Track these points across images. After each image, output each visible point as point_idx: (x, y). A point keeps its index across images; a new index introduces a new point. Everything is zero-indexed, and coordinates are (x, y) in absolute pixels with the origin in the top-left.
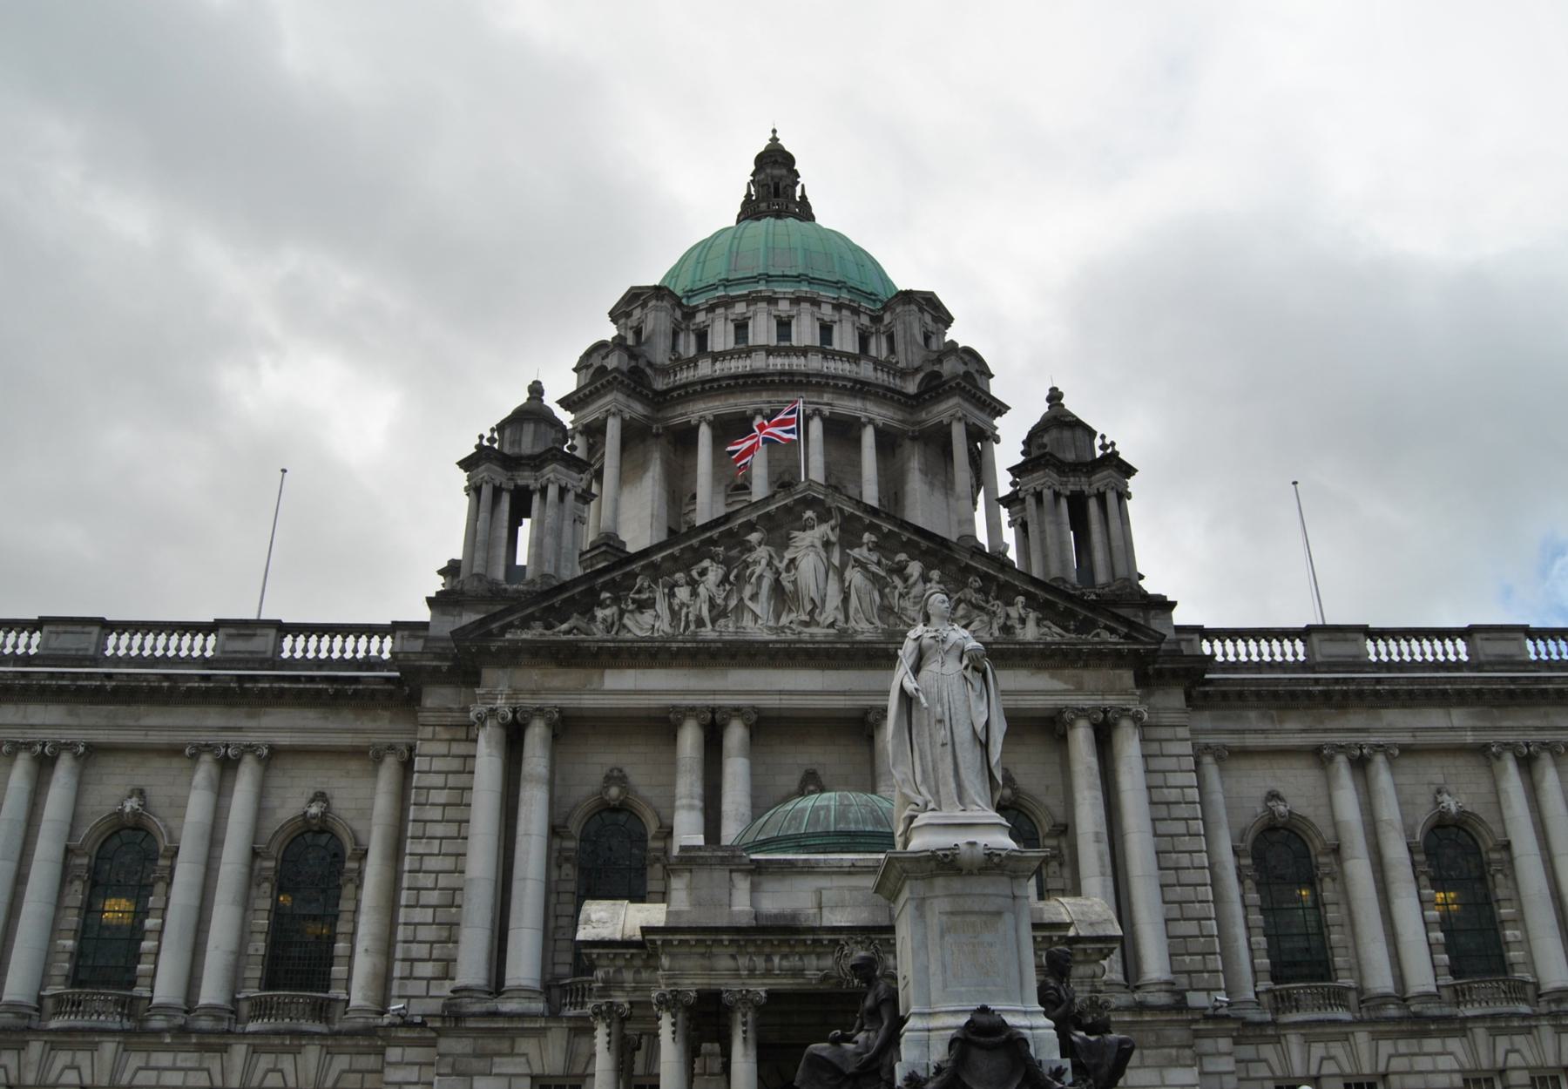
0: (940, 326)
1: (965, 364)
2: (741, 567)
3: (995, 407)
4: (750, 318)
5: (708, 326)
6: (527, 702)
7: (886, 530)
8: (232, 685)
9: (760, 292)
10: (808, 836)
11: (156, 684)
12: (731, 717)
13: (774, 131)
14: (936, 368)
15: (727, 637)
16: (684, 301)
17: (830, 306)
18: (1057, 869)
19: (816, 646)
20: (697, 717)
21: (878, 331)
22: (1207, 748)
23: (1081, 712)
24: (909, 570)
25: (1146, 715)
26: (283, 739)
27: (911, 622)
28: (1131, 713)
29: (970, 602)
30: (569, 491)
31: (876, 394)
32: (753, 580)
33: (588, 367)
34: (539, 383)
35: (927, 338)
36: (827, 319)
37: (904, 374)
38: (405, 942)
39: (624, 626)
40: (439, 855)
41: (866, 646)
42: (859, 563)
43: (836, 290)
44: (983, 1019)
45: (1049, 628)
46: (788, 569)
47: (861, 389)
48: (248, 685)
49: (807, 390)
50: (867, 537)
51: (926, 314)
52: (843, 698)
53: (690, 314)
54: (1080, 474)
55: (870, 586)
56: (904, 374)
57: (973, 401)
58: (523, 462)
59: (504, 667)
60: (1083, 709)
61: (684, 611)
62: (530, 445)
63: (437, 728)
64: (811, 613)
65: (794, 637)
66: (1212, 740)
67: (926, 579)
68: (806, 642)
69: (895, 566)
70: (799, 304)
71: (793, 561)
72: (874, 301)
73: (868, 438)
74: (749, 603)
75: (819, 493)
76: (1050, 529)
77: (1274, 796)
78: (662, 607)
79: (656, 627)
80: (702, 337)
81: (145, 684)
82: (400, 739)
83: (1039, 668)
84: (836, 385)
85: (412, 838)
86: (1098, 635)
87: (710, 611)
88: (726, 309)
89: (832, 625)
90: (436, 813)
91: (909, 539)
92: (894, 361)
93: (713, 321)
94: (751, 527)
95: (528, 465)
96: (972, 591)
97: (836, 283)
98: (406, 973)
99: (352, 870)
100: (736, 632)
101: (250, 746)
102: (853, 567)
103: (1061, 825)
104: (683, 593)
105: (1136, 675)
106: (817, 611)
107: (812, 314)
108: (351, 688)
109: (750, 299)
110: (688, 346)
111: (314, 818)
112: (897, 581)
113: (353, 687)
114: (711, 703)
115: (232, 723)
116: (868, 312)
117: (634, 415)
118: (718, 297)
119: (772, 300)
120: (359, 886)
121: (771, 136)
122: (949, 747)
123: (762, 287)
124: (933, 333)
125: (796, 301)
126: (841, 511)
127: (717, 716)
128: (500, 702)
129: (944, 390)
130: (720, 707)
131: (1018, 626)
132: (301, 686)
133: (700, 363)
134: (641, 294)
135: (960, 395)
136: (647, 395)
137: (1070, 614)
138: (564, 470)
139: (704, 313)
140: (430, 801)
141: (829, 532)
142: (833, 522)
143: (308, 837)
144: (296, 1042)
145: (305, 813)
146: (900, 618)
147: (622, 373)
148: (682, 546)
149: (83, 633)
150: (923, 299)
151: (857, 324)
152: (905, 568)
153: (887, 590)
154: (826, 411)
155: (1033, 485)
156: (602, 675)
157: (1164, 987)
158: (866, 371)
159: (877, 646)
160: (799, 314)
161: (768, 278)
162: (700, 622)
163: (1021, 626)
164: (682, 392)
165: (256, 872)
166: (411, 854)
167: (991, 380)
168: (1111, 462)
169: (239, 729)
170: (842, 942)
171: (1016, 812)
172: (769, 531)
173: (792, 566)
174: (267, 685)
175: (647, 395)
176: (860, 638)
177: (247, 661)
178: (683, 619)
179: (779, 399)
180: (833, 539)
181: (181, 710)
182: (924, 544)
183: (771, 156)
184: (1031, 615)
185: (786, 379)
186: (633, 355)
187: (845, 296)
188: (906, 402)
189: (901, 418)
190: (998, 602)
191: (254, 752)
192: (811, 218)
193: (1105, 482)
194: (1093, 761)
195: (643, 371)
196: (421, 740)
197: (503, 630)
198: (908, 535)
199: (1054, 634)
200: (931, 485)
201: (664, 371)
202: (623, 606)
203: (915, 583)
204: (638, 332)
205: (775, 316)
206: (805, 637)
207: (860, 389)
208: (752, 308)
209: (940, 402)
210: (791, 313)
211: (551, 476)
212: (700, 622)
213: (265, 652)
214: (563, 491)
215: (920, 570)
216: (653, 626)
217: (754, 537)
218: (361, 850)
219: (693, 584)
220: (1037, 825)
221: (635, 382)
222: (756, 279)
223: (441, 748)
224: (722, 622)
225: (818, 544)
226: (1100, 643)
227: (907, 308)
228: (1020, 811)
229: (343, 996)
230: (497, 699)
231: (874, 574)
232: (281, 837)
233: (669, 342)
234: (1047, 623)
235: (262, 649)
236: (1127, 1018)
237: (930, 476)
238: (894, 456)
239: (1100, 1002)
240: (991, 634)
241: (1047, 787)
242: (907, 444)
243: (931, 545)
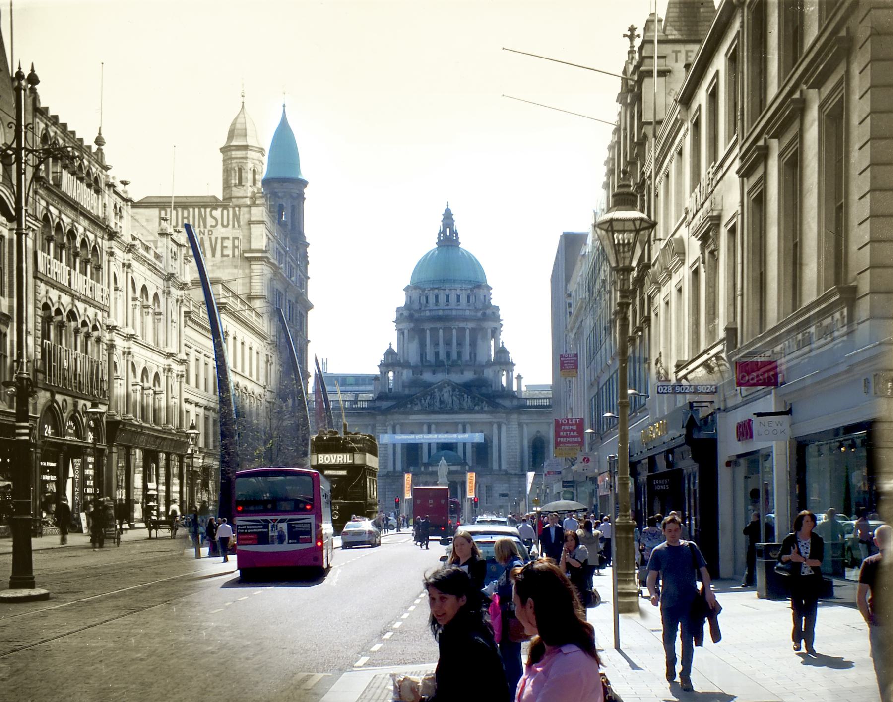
6: (396, 422)
22: (525, 423)
35: (485, 296)
37: (477, 310)
66: (527, 421)
73: (468, 331)
77: (538, 432)
78: (419, 404)
80: (427, 298)
82: (371, 423)
94: (435, 388)
104: (423, 401)
110: (423, 300)
125: (451, 289)
187: (464, 286)
194: (497, 432)
217: (436, 390)
219: (425, 400)
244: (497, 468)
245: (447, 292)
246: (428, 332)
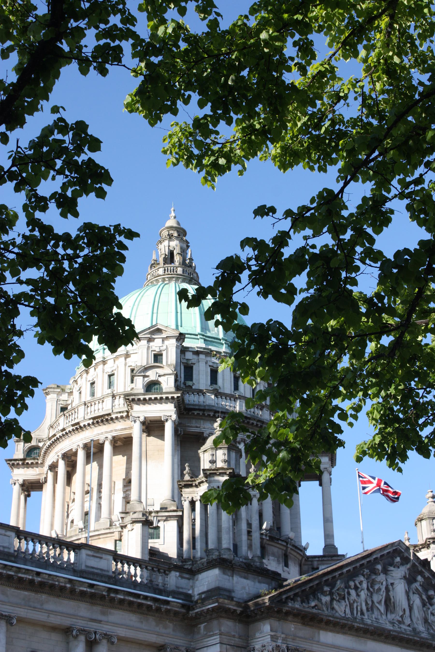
5: (194, 364)
7: (426, 576)
8: (104, 593)
11: (63, 584)
26: (122, 632)
39: (333, 609)
42: (417, 592)
48: (112, 595)
50: (419, 578)
59: (279, 621)
61: (355, 605)
65: (399, 630)
71: (392, 584)
74: (377, 605)
81: (57, 583)
89: (409, 626)
102: (414, 593)
113: (165, 607)
115: (94, 617)
128: (279, 642)
132: (139, 601)
139: (191, 353)
146: (431, 626)
149: (5, 535)
156: (319, 633)
162: (362, 613)
164: (201, 413)
169: (100, 622)
174: (122, 597)
181: (66, 602)
202: (334, 597)
213: (108, 571)
219: (356, 588)
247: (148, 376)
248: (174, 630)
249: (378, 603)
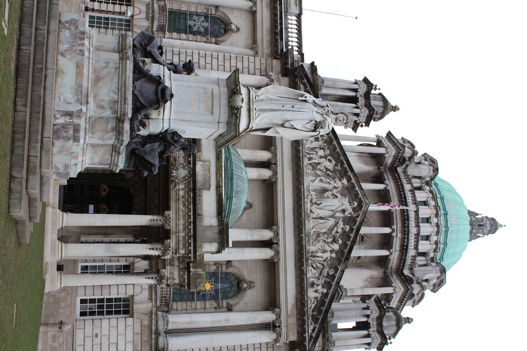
0: (432, 287)
1: (418, 294)
2: (333, 176)
3: (400, 307)
4: (429, 207)
7: (351, 235)
9: (440, 211)
10: (231, 163)
12: (273, 171)
13: (505, 226)
14: (415, 282)
15: (305, 168)
16: (433, 182)
17: (436, 240)
18: (214, 306)
19: (303, 204)
20: (273, 157)
21: (427, 260)
23: (279, 316)
24: (335, 244)
25: (278, 344)
27: (314, 244)
28: (279, 338)
29: (323, 269)
30: (358, 117)
31: (402, 256)
32: (328, 180)
33: (404, 142)
34: (398, 110)
35: (427, 281)
36: (431, 238)
37: (411, 269)
38: (186, 52)
40: (218, 64)
41: (303, 224)
42: (337, 223)
43: (443, 243)
44: (168, 92)
45: (314, 303)
46: (333, 195)
47: (403, 249)
49: (402, 226)
50: (348, 227)
51: (437, 280)
52: (282, 216)
53: (428, 183)
54: (378, 327)
55: (328, 228)
56: (411, 269)
57: (402, 297)
58: (368, 100)
60: (280, 317)
61: (315, 153)
62: (374, 104)
63: (265, 65)
64: (316, 203)
65: (306, 195)
67: (332, 251)
68: (304, 200)
69: (336, 239)
70: (436, 227)
71: (336, 197)
72: (440, 260)
73: (385, 253)
75: (364, 208)
76: (354, 313)
78: (316, 144)
79: (308, 141)
80: (420, 188)
83: (297, 299)
84: (405, 238)
85: (224, 55)
86: (312, 324)
87: (314, 163)
88: (432, 198)
89: (311, 212)
90: (233, 64)
91: (348, 244)
92: (416, 266)
93: (426, 192)
94: (349, 180)
95: (367, 102)
96: (327, 270)
97: (446, 243)
98: (174, 52)
99: (211, 40)
100: (307, 173)
101: (256, 4)
103: (232, 308)
104: (321, 153)
105: (295, 341)
106: (317, 206)
107: (433, 232)
108: (278, 37)
109: (436, 207)
110: (416, 183)
111: (230, 26)
112: (330, 240)
113: (279, 38)
114: (279, 163)
116: (435, 256)
117: (386, 159)
118: (436, 194)
119: (437, 215)
120: (205, 42)
121: (503, 224)
122: (282, 108)
123: (442, 212)
124: (428, 284)
125: (438, 225)
126: (358, 217)
127: (273, 165)
129: (406, 284)
130: (277, 166)
131: (314, 289)
132: (279, 20)
133: (409, 185)
134: (435, 164)
135: (404, 291)
136: (395, 164)
137: (320, 312)
138: (366, 116)
139: (430, 189)
140: (238, 62)
141: (349, 212)
142: (353, 213)
143: (223, 26)
144: (150, 18)
145: (232, 23)
146: (315, 240)
147: (403, 153)
148: (340, 152)
150: (443, 279)
151: (429, 252)
152: (336, 243)
153: (326, 235)
154: (394, 234)
155: (372, 306)
157: (166, 343)
158: (411, 252)
159: (304, 229)
160: (432, 226)
161: (446, 214)
162: (310, 159)
163: (314, 291)
165: (210, 7)
166: (218, 55)
167: (411, 307)
168: (384, 340)
170: (189, 165)
171: (237, 291)
172: (347, 188)
173: (334, 197)
174: (278, 9)
175: (395, 164)
176: (307, 222)
177: (287, 3)
178: (311, 152)
179: (398, 216)
180: (346, 213)
182: (346, 251)
183: (494, 223)
184: (319, 295)
185: (406, 217)
186: (411, 158)
187: (442, 246)
188: (399, 269)
189: (393, 267)
190: (323, 281)
191: (254, 5)
192: (471, 239)
193: (375, 337)
195: (404, 163)
196: (261, 59)
197: (304, 84)
198: (349, 245)
199: (311, 305)
200: (366, 281)
201: (405, 172)
203: (329, 246)
204: (419, 163)
205: (430, 217)
206: (306, 200)
207: (404, 249)
208: (433, 208)
209: (401, 283)
210: (432, 223)
211: (363, 110)
212: (310, 159)
213: (290, 9)
214: (357, 115)
215: (335, 249)
216: (308, 141)
217: (345, 181)
218: (219, 43)
220: (232, 299)
221: (400, 159)
222: (444, 209)
223: (258, 66)
224: (311, 168)
225: (343, 207)
226: (308, 324)
227: (439, 271)
228: (237, 292)
229: (166, 36)
230: (277, 82)
231: (333, 229)
232: (223, 16)
233: (416, 174)
234: (315, 303)
235: (291, 8)
236: (153, 328)
237: (370, 280)
238: (377, 265)
239: (163, 280)
240: (310, 278)
241: (247, 304)
242: (382, 270)
243: (346, 253)
244: (170, 327)
245: (434, 220)
246: (380, 187)
247: (405, 143)
248: (266, 53)
249: (320, 179)
